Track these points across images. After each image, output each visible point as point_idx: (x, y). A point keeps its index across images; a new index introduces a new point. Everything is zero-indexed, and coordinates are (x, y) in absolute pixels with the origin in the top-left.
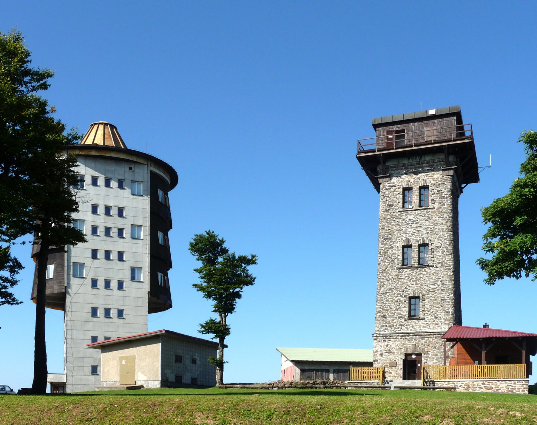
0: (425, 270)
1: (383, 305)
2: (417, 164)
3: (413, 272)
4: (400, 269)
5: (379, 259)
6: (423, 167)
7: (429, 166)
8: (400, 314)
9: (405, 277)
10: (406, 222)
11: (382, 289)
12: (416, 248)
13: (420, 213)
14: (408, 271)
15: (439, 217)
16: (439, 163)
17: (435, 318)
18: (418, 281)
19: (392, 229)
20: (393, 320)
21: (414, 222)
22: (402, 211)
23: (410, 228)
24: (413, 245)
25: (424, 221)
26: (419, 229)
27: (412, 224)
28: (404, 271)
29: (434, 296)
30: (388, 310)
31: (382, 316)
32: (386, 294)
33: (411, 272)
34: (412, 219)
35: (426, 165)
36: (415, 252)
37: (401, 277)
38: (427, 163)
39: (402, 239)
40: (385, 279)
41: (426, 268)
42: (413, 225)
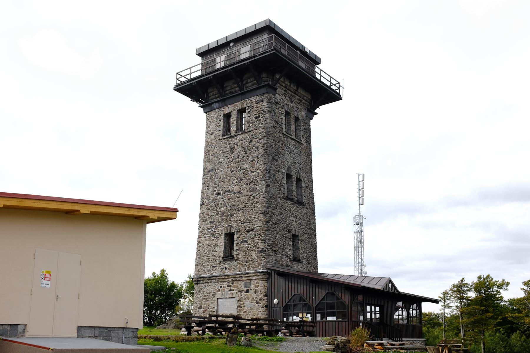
0: (300, 208)
1: (274, 237)
2: (295, 93)
3: (293, 207)
4: (285, 199)
5: (269, 179)
6: (295, 97)
7: (299, 100)
8: (286, 253)
9: (289, 210)
10: (287, 148)
11: (273, 217)
12: (295, 181)
13: (295, 143)
14: (290, 204)
15: (306, 156)
16: (305, 102)
17: (308, 264)
18: (297, 218)
19: (278, 150)
20: (282, 258)
21: (292, 152)
22: (285, 135)
23: (289, 156)
24: (293, 176)
25: (298, 155)
26: (295, 161)
27: (291, 152)
28: (287, 202)
29: (306, 239)
30: (278, 245)
31: (274, 251)
32: (276, 225)
33: (292, 206)
34: (290, 147)
35: (297, 97)
36: (295, 185)
37: (285, 208)
38: (300, 97)
39: (285, 166)
40: (274, 205)
41: (300, 206)
42: (292, 155)
